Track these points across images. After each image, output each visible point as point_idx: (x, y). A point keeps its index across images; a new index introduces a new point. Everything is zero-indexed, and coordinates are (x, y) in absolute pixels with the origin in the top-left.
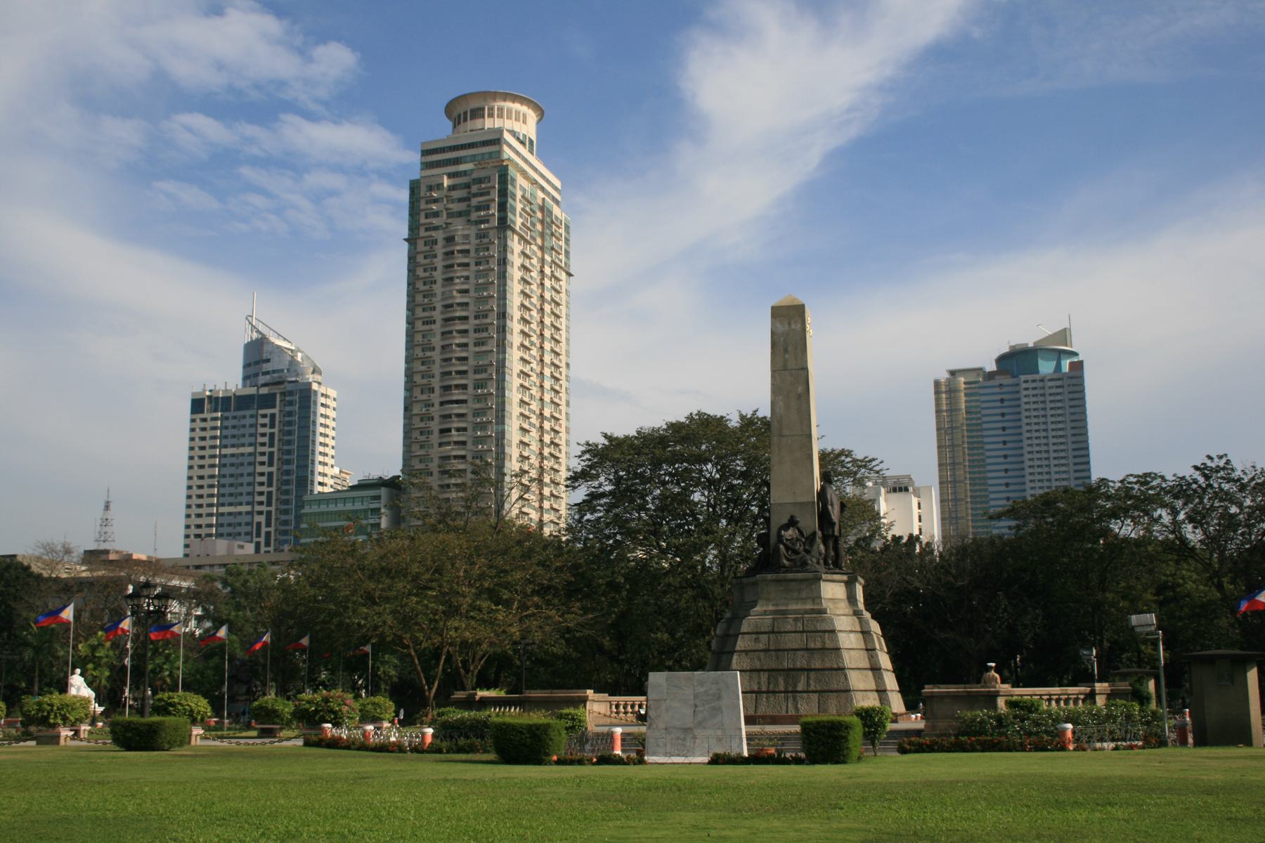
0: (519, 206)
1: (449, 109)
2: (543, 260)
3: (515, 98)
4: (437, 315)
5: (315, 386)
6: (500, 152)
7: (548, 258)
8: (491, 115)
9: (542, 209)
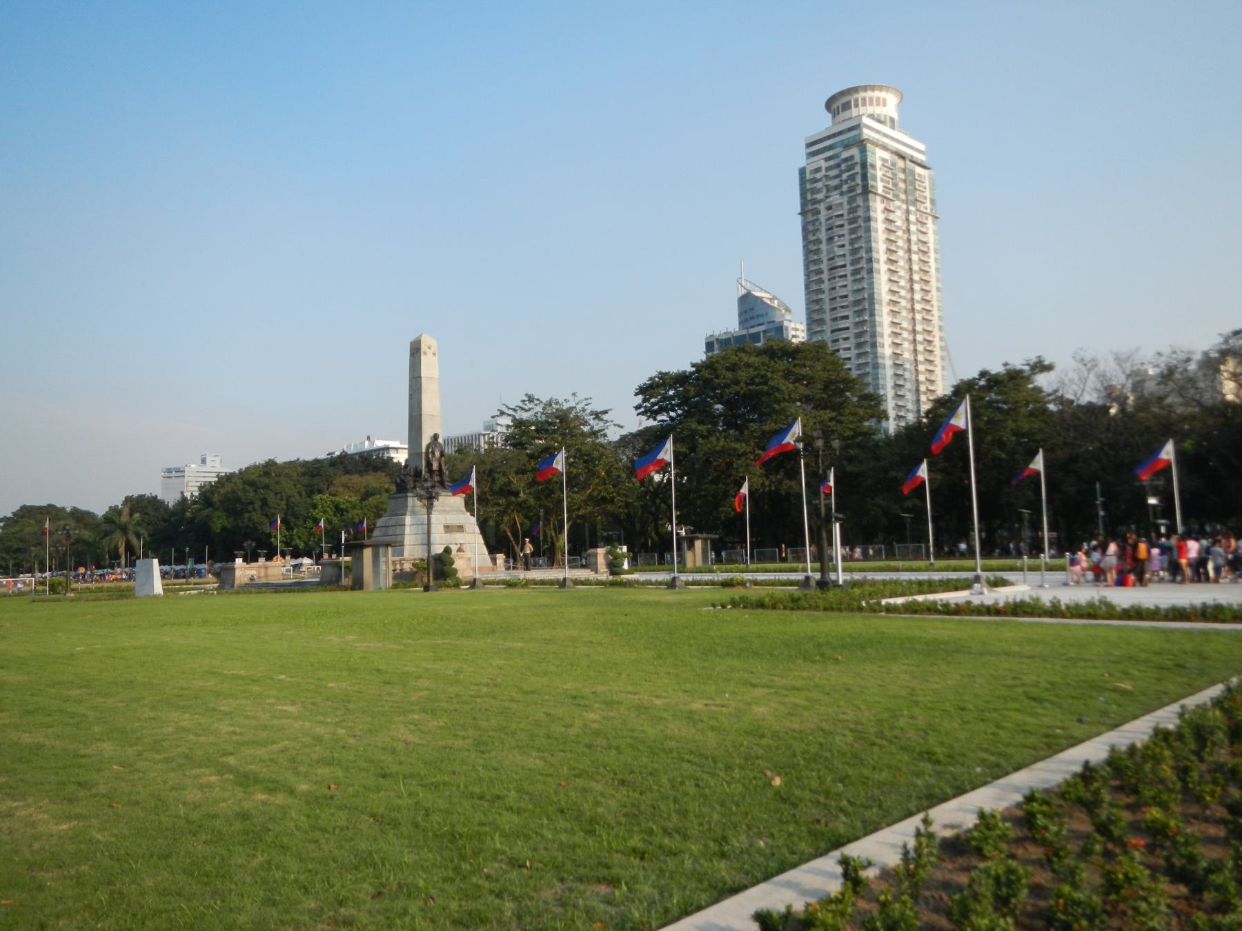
0: (879, 174)
1: (829, 105)
2: (908, 212)
3: (873, 88)
4: (825, 266)
5: (786, 323)
6: (860, 134)
7: (912, 208)
8: (857, 106)
9: (904, 171)
